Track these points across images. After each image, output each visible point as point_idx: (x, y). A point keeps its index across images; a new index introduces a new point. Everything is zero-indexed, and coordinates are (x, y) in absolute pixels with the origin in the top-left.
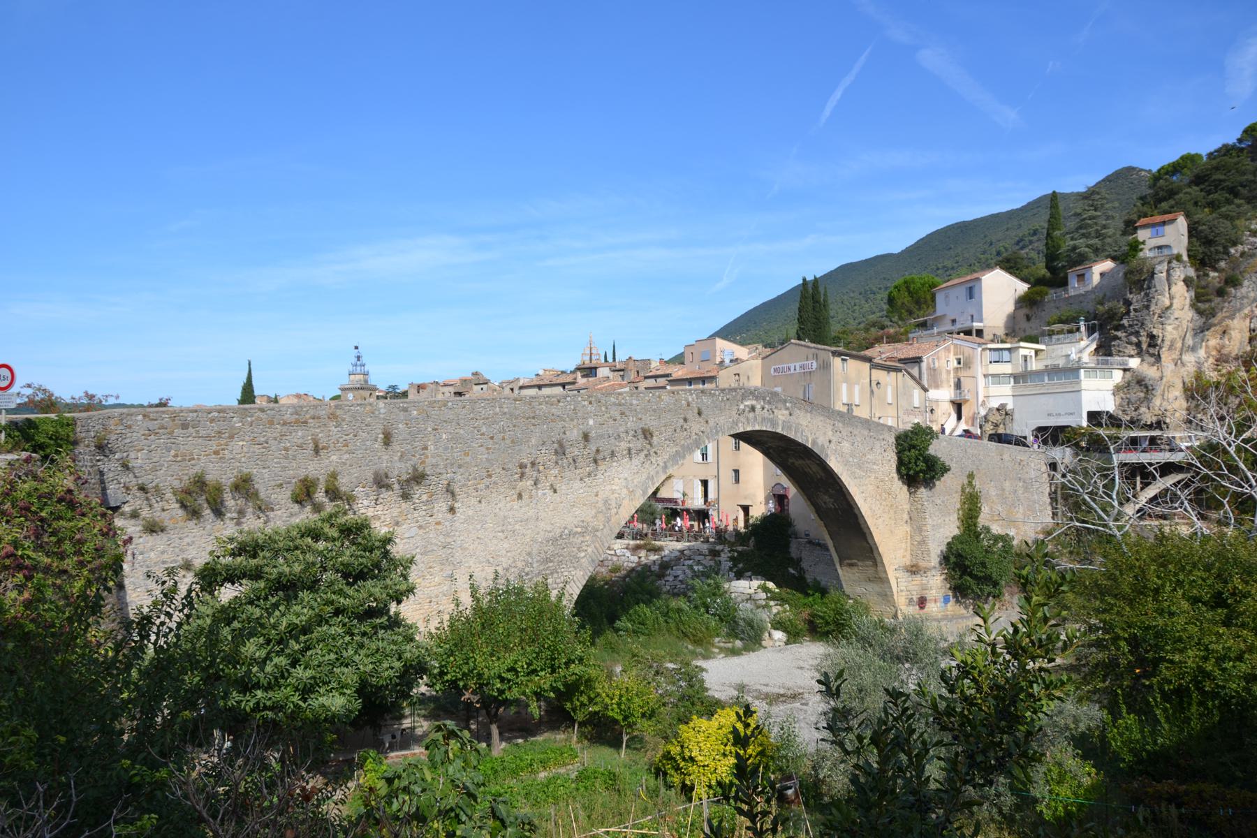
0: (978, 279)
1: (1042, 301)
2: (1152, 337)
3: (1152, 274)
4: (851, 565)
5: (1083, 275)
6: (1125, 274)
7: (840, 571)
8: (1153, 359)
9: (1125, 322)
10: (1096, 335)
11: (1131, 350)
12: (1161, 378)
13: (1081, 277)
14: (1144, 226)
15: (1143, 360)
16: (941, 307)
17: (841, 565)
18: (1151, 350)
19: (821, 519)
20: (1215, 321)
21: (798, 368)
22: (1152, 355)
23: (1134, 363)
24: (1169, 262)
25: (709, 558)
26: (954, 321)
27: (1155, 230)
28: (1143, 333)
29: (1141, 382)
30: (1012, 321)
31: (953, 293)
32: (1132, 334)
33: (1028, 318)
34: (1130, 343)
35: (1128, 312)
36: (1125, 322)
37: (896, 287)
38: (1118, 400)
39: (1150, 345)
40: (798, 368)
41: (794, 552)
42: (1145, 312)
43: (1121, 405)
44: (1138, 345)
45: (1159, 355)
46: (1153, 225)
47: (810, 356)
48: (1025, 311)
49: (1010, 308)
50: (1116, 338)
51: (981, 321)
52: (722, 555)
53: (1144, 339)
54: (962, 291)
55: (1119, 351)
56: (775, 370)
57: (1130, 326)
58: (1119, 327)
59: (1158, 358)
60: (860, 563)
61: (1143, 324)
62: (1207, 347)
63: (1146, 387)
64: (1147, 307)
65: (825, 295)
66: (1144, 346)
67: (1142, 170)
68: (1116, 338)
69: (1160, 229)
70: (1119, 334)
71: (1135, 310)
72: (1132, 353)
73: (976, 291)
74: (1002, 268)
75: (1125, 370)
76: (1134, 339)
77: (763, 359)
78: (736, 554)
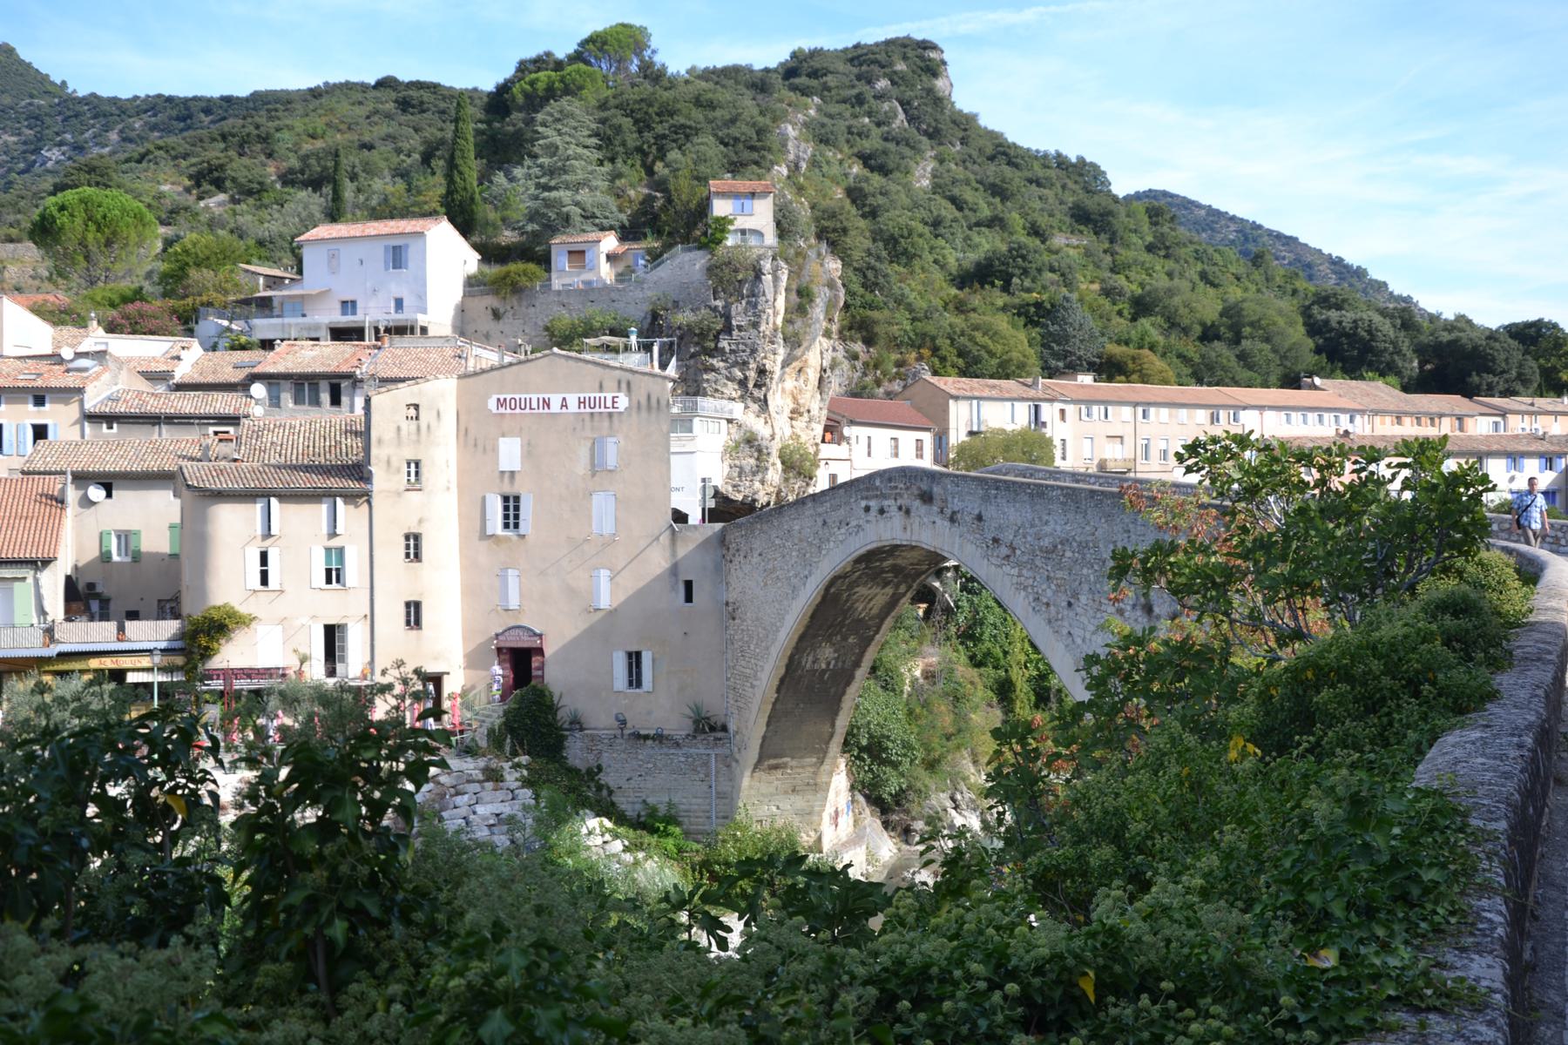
0: (421, 235)
1: (533, 288)
2: (762, 372)
3: (758, 274)
4: (776, 767)
5: (583, 252)
6: (711, 270)
7: (746, 782)
8: (755, 407)
9: (724, 344)
10: (674, 360)
11: (731, 389)
12: (773, 437)
13: (577, 255)
14: (723, 195)
15: (746, 407)
16: (316, 273)
17: (754, 771)
18: (758, 393)
19: (778, 691)
20: (798, 352)
21: (573, 406)
22: (755, 400)
23: (737, 409)
24: (774, 259)
25: (489, 785)
26: (348, 306)
27: (739, 203)
28: (753, 365)
29: (750, 440)
30: (462, 310)
31: (349, 254)
32: (735, 364)
33: (497, 315)
34: (730, 379)
35: (728, 329)
36: (724, 344)
37: (62, 208)
38: (727, 470)
39: (755, 386)
40: (573, 406)
41: (576, 753)
42: (753, 332)
43: (729, 477)
44: (743, 383)
45: (766, 400)
46: (735, 195)
47: (610, 383)
48: (491, 301)
49: (456, 293)
50: (713, 369)
51: (424, 311)
52: (507, 777)
53: (752, 375)
54: (378, 252)
55: (716, 390)
57: (732, 351)
58: (716, 352)
59: (764, 403)
60: (794, 763)
61: (754, 351)
62: (783, 390)
63: (760, 451)
64: (755, 325)
66: (751, 385)
68: (713, 369)
69: (747, 203)
70: (715, 362)
71: (740, 328)
72: (734, 395)
73: (412, 254)
74: (452, 220)
75: (730, 421)
76: (738, 374)
77: (460, 377)
78: (525, 773)
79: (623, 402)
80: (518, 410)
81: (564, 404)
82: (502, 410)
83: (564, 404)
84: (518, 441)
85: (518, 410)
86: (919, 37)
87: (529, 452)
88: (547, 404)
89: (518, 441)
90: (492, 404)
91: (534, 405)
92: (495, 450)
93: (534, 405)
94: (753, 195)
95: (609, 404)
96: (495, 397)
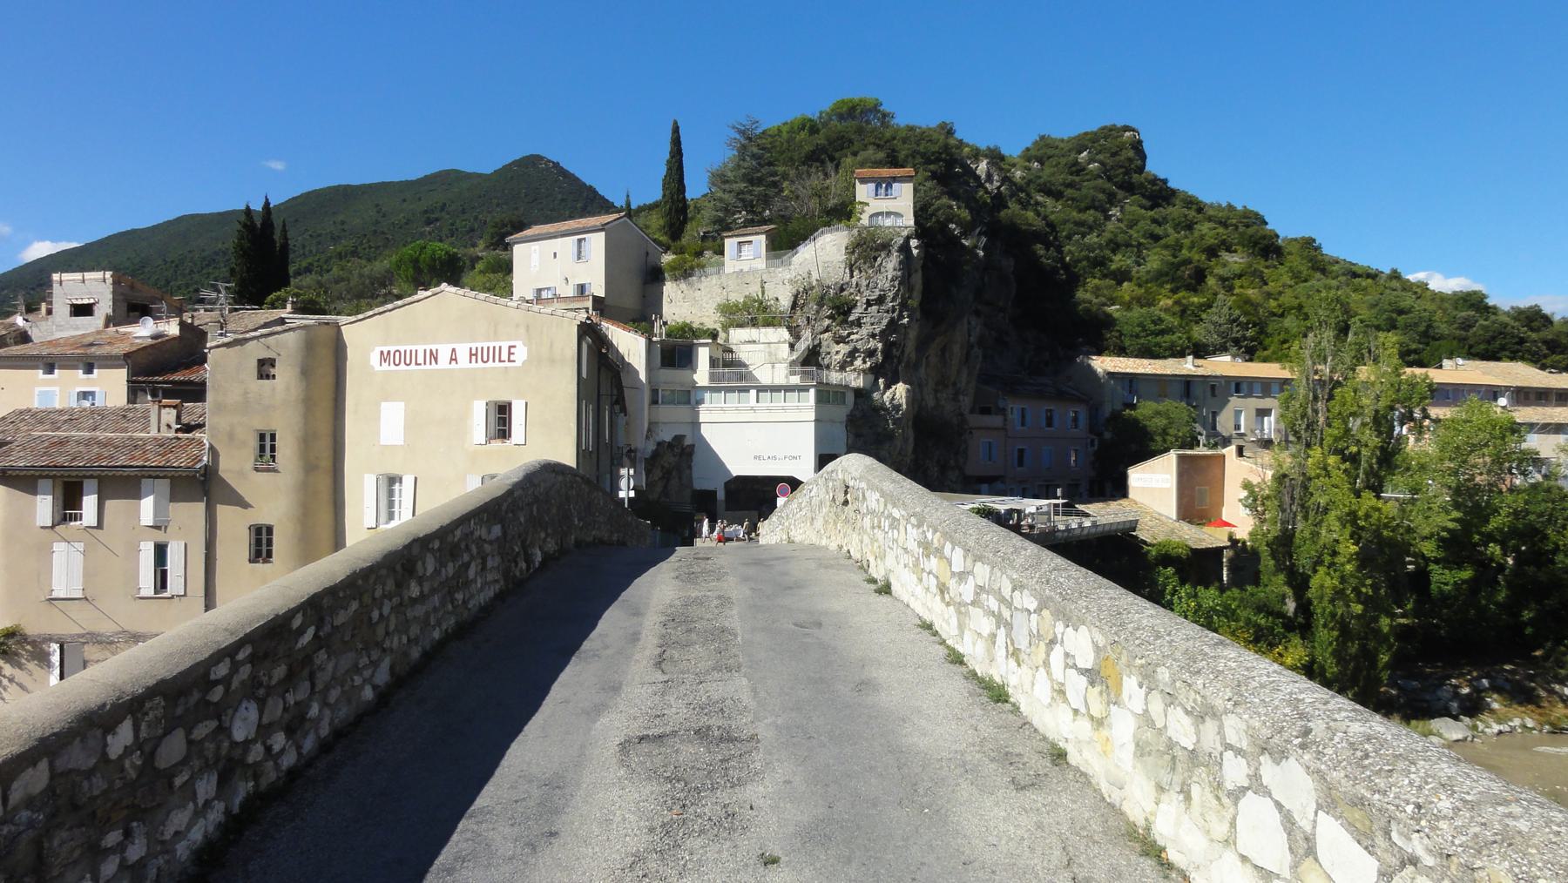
14: (864, 181)
21: (463, 355)
40: (463, 355)
56: (384, 357)
62: (928, 365)
65: (284, 230)
67: (550, 161)
79: (521, 354)
80: (403, 366)
81: (453, 359)
82: (385, 365)
83: (453, 359)
84: (402, 405)
85: (403, 366)
86: (1120, 124)
87: (412, 425)
88: (434, 357)
89: (402, 405)
90: (375, 358)
91: (421, 360)
92: (377, 419)
93: (421, 360)
94: (895, 179)
95: (505, 356)
96: (378, 350)
